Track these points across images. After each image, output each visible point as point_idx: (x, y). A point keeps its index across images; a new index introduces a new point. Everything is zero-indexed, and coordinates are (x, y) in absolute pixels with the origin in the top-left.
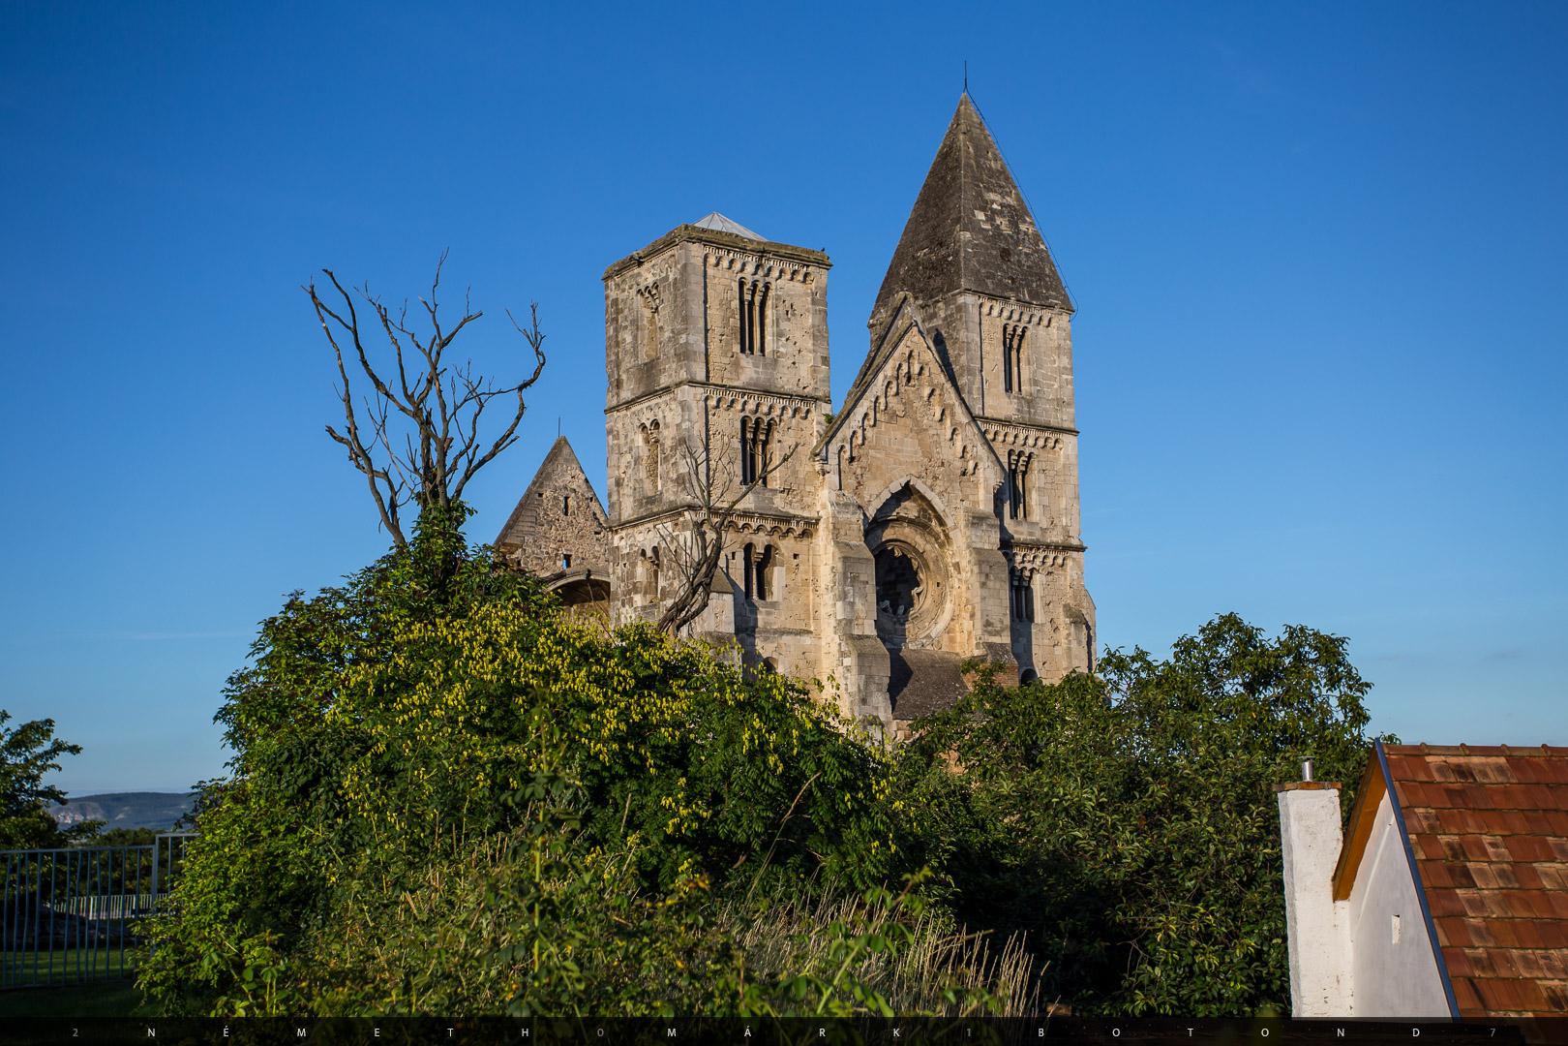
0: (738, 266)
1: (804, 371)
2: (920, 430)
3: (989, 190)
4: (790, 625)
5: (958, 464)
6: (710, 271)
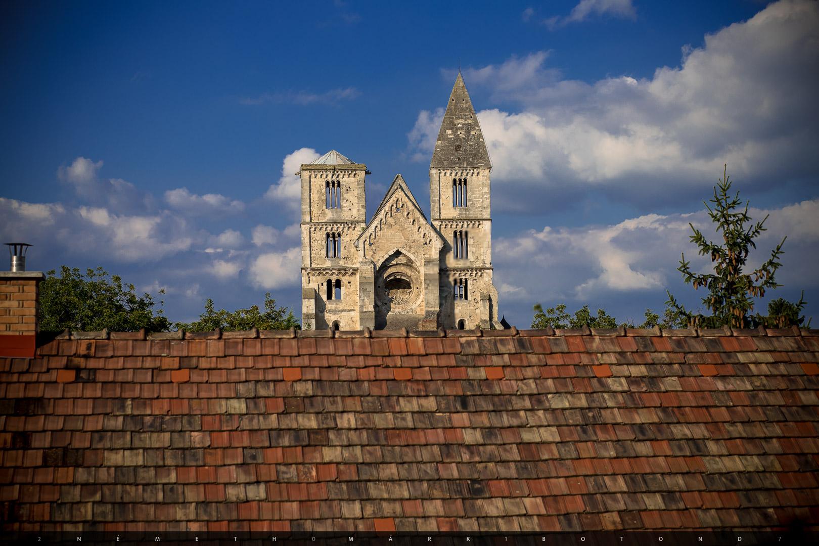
0: (324, 176)
1: (354, 212)
2: (403, 229)
3: (457, 118)
4: (347, 308)
5: (423, 240)
6: (312, 180)
